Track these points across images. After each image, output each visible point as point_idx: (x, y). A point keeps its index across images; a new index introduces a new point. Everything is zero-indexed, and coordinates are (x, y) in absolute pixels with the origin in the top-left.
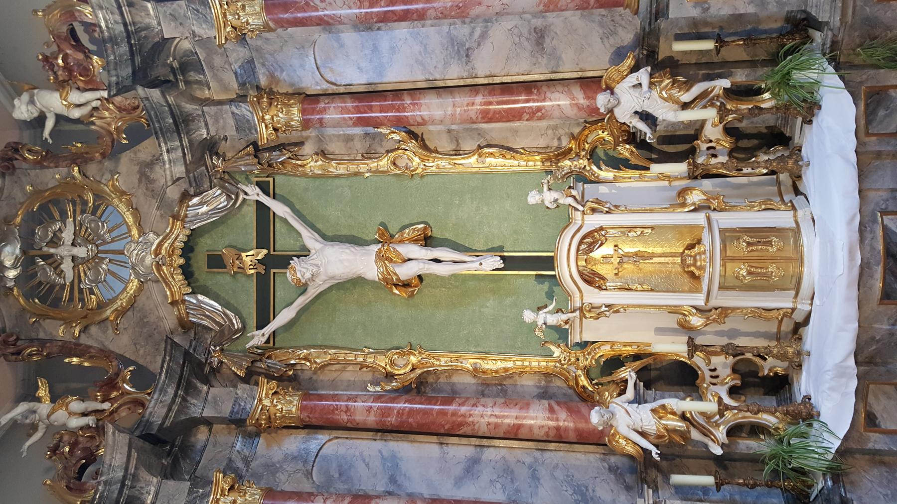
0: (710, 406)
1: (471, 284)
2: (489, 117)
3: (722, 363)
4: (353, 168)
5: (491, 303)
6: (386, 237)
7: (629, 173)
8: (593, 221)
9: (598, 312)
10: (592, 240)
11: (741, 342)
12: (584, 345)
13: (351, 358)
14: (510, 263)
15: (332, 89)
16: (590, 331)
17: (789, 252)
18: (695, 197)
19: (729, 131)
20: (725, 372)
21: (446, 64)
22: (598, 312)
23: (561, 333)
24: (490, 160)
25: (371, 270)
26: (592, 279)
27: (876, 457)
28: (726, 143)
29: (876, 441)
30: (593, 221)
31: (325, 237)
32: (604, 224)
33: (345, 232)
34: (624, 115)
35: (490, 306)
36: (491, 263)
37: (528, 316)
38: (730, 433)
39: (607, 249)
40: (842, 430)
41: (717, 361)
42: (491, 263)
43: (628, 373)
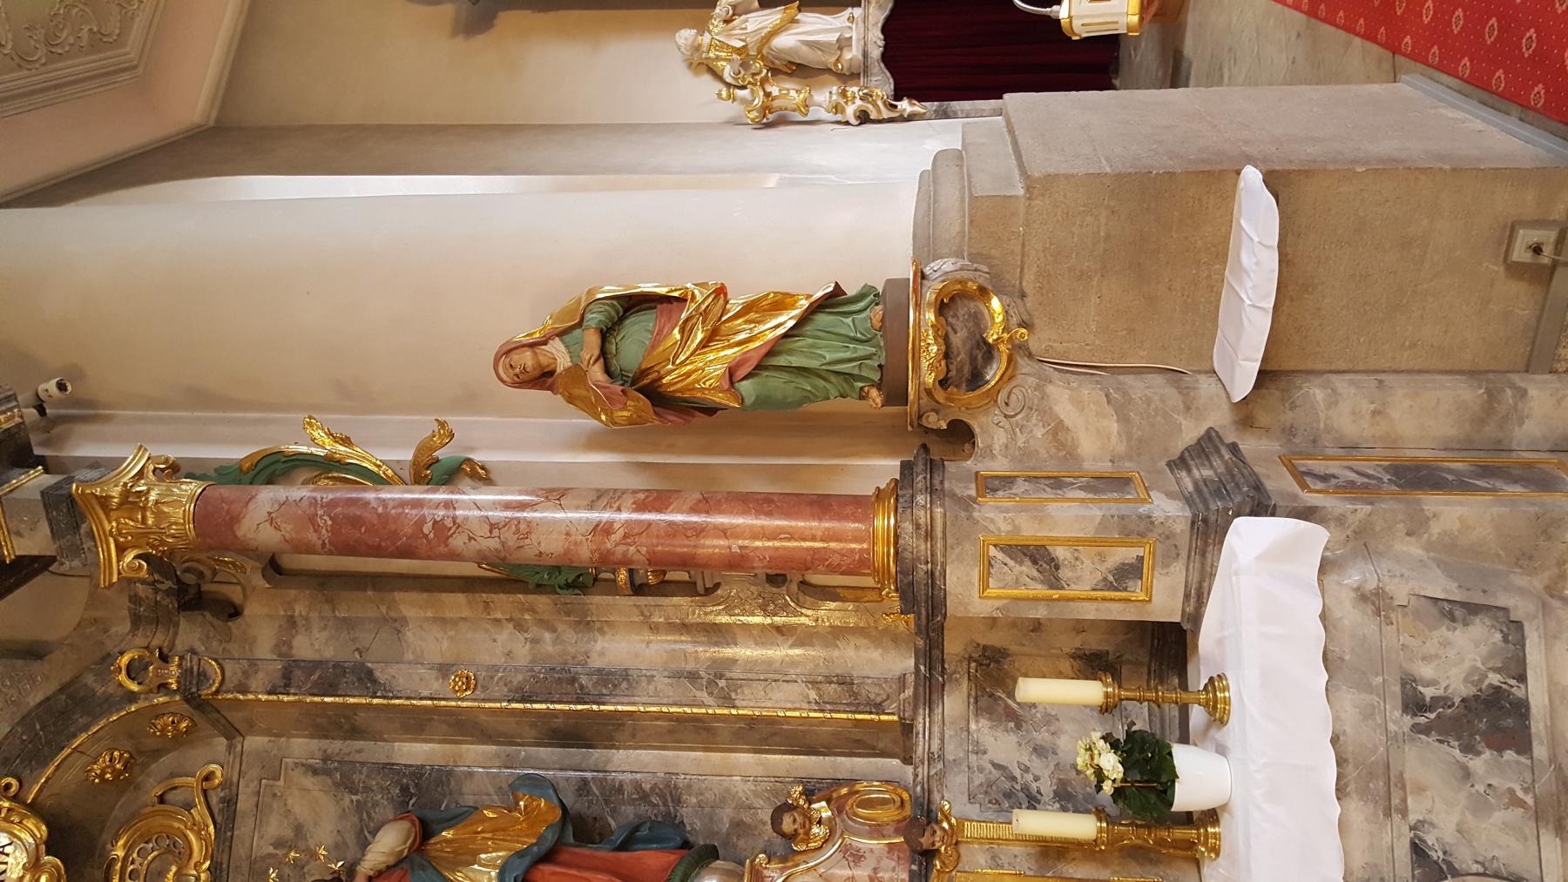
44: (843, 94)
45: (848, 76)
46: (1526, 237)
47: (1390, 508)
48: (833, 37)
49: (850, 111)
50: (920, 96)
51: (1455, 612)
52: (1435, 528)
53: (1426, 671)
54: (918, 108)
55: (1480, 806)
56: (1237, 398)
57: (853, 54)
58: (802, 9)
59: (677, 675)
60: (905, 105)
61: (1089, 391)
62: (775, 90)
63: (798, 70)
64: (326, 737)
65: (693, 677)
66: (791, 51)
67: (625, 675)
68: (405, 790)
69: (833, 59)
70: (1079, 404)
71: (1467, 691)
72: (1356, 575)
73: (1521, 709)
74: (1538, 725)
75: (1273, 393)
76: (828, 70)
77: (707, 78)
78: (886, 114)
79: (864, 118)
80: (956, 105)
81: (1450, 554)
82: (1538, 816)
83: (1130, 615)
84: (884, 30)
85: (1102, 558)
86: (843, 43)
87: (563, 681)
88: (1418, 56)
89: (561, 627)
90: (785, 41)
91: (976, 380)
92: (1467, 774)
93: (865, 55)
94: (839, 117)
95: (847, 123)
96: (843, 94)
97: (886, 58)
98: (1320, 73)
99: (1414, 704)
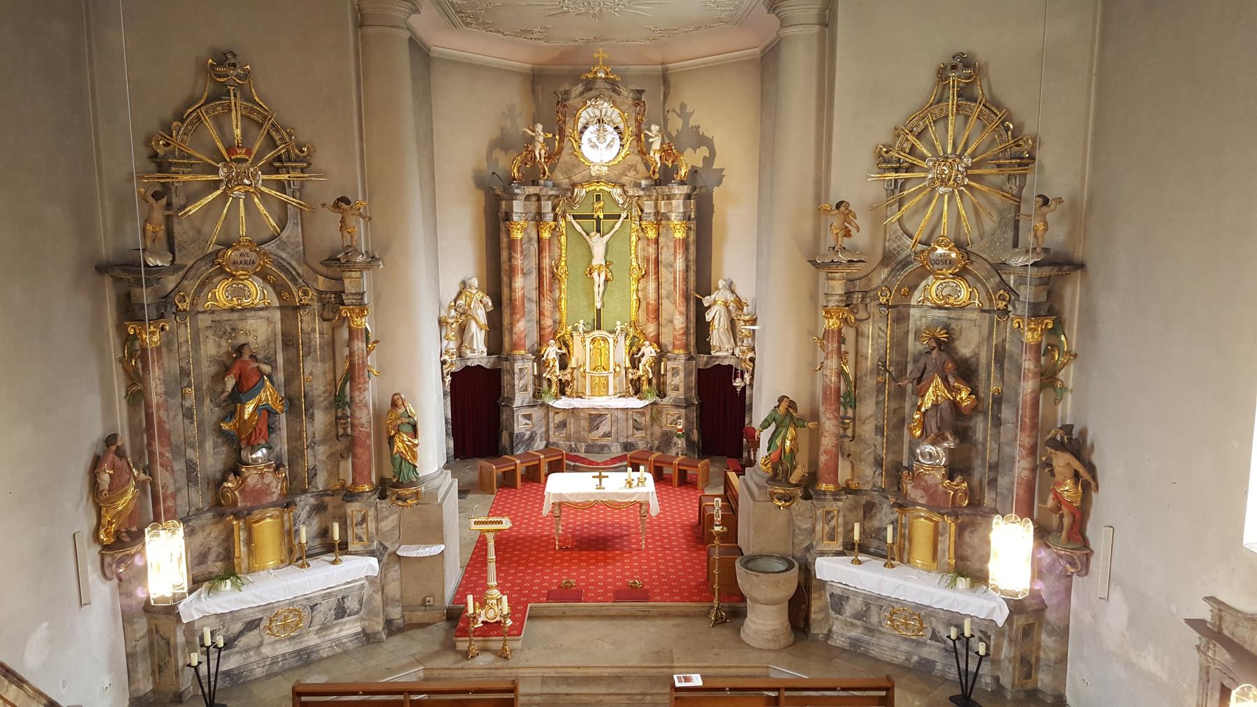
0: (558, 373)
1: (591, 296)
2: (648, 304)
3: (568, 377)
4: (633, 252)
5: (585, 303)
6: (608, 264)
7: (628, 350)
8: (611, 341)
9: (583, 341)
10: (605, 340)
11: (575, 382)
12: (572, 336)
13: (564, 251)
14: (599, 311)
15: (660, 248)
16: (577, 339)
17: (602, 393)
18: (618, 369)
19: (639, 379)
20: (566, 378)
21: (666, 290)
22: (583, 341)
23: (575, 329)
24: (635, 302)
25: (595, 263)
26: (593, 341)
27: (547, 414)
28: (635, 377)
29: (551, 414)
30: (611, 341)
31: (607, 244)
32: (577, 406)
33: (610, 248)
34: (643, 349)
35: (584, 303)
36: (598, 305)
37: (582, 321)
38: (549, 379)
39: (602, 345)
40: (554, 405)
41: (569, 375)
42: (598, 305)
43: (564, 350)
44: (453, 354)
45: (461, 356)
46: (431, 599)
47: (379, 586)
48: (475, 347)
49: (446, 357)
50: (452, 384)
51: (361, 602)
52: (375, 595)
53: (349, 599)
54: (447, 383)
55: (325, 613)
56: (398, 553)
57: (469, 354)
58: (459, 611)
59: (314, 433)
60: (449, 378)
61: (395, 523)
62: (454, 326)
63: (463, 329)
64: (282, 334)
65: (314, 437)
66: (469, 329)
67: (313, 420)
68: (270, 358)
69: (466, 345)
70: (392, 521)
71: (346, 606)
72: (367, 584)
73: (343, 617)
74: (339, 621)
75: (397, 558)
76: (462, 343)
77: (458, 289)
78: (445, 372)
79: (444, 363)
80: (449, 399)
81: (371, 598)
82: (323, 624)
83: (349, 541)
84: (478, 365)
85: (364, 534)
86: (473, 351)
87: (310, 405)
88: (466, 572)
89: (326, 402)
90: (473, 326)
91: (398, 499)
92: (330, 610)
93: (468, 359)
94: (443, 352)
95: (441, 356)
96: (453, 354)
97: (468, 367)
98: (462, 547)
99: (343, 598)
